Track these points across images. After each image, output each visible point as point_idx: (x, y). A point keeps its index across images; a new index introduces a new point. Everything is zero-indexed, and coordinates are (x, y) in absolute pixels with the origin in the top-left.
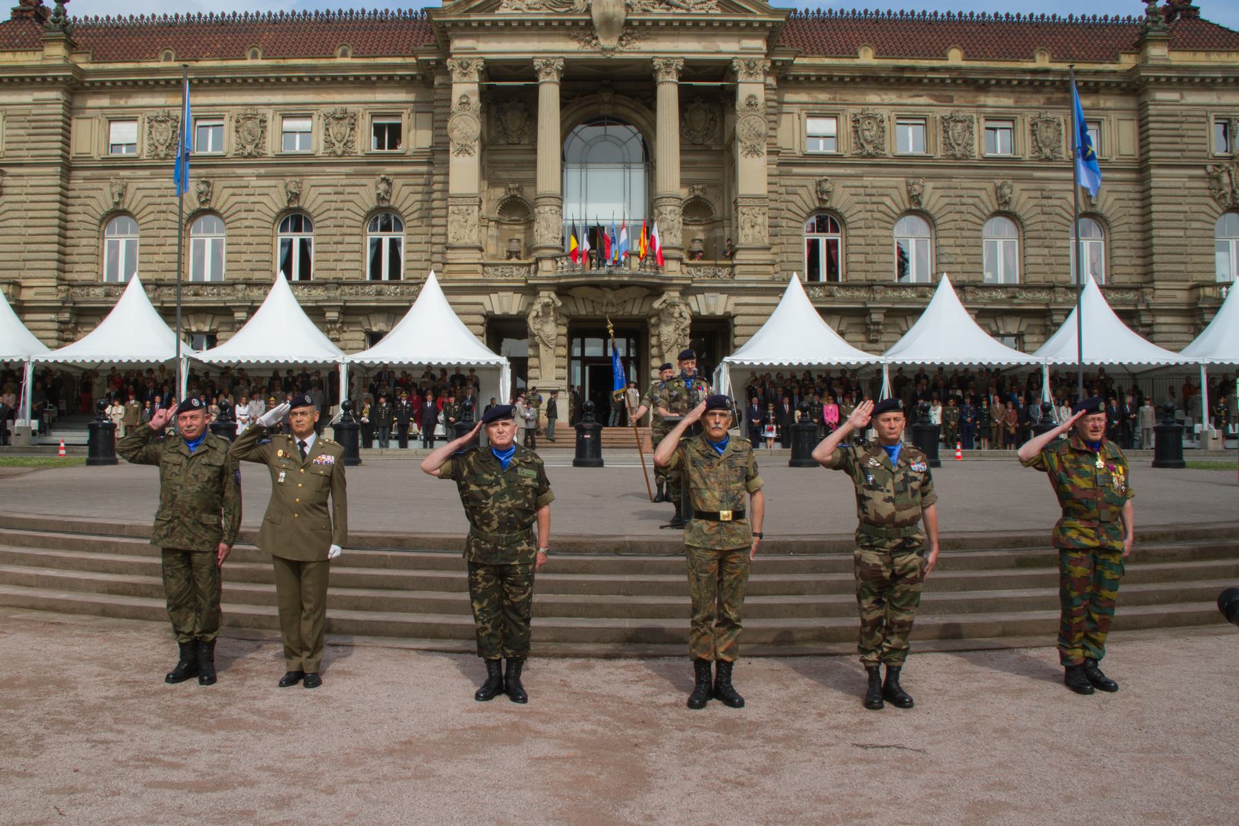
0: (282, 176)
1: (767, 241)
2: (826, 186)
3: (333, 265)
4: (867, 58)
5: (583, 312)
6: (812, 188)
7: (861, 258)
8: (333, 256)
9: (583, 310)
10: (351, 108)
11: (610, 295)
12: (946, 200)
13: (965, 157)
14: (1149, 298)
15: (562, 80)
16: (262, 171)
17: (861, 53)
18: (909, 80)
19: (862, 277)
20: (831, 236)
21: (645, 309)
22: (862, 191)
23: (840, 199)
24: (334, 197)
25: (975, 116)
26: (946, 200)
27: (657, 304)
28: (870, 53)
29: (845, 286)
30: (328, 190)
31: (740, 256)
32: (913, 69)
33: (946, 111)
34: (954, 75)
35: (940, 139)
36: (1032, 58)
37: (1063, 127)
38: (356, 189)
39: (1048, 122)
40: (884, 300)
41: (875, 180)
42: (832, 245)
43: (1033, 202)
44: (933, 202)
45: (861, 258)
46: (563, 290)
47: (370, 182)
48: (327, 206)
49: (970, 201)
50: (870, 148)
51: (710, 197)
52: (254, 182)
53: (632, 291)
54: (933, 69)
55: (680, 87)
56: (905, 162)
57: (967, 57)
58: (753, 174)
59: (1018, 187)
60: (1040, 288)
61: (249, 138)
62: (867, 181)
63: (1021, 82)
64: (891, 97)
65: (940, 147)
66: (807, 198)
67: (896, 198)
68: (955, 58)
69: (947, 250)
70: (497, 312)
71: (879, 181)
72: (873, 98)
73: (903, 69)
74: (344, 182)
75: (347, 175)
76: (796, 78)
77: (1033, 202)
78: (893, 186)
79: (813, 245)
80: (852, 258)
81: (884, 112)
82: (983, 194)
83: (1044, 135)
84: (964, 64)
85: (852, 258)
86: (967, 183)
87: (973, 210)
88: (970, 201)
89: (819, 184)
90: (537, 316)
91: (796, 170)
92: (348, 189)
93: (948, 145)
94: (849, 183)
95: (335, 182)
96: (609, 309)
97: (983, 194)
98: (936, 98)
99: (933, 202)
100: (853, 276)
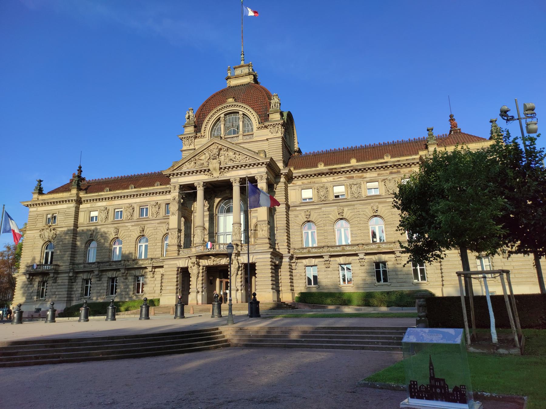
6: (303, 214)
10: (159, 202)
12: (353, 214)
15: (205, 189)
16: (133, 224)
17: (319, 165)
18: (335, 173)
22: (322, 213)
25: (362, 182)
26: (353, 214)
28: (323, 165)
32: (336, 169)
33: (351, 181)
34: (352, 168)
35: (349, 192)
41: (326, 209)
43: (387, 211)
44: (348, 214)
49: (362, 213)
50: (323, 198)
54: (343, 168)
57: (357, 161)
59: (380, 206)
60: (391, 243)
63: (377, 168)
64: (330, 178)
65: (349, 194)
68: (353, 162)
69: (354, 232)
71: (328, 209)
72: (324, 179)
73: (332, 169)
77: (387, 211)
78: (333, 211)
82: (367, 210)
83: (389, 185)
84: (357, 164)
86: (361, 207)
87: (364, 216)
88: (362, 213)
91: (298, 208)
97: (367, 210)
98: (348, 178)
99: (348, 214)
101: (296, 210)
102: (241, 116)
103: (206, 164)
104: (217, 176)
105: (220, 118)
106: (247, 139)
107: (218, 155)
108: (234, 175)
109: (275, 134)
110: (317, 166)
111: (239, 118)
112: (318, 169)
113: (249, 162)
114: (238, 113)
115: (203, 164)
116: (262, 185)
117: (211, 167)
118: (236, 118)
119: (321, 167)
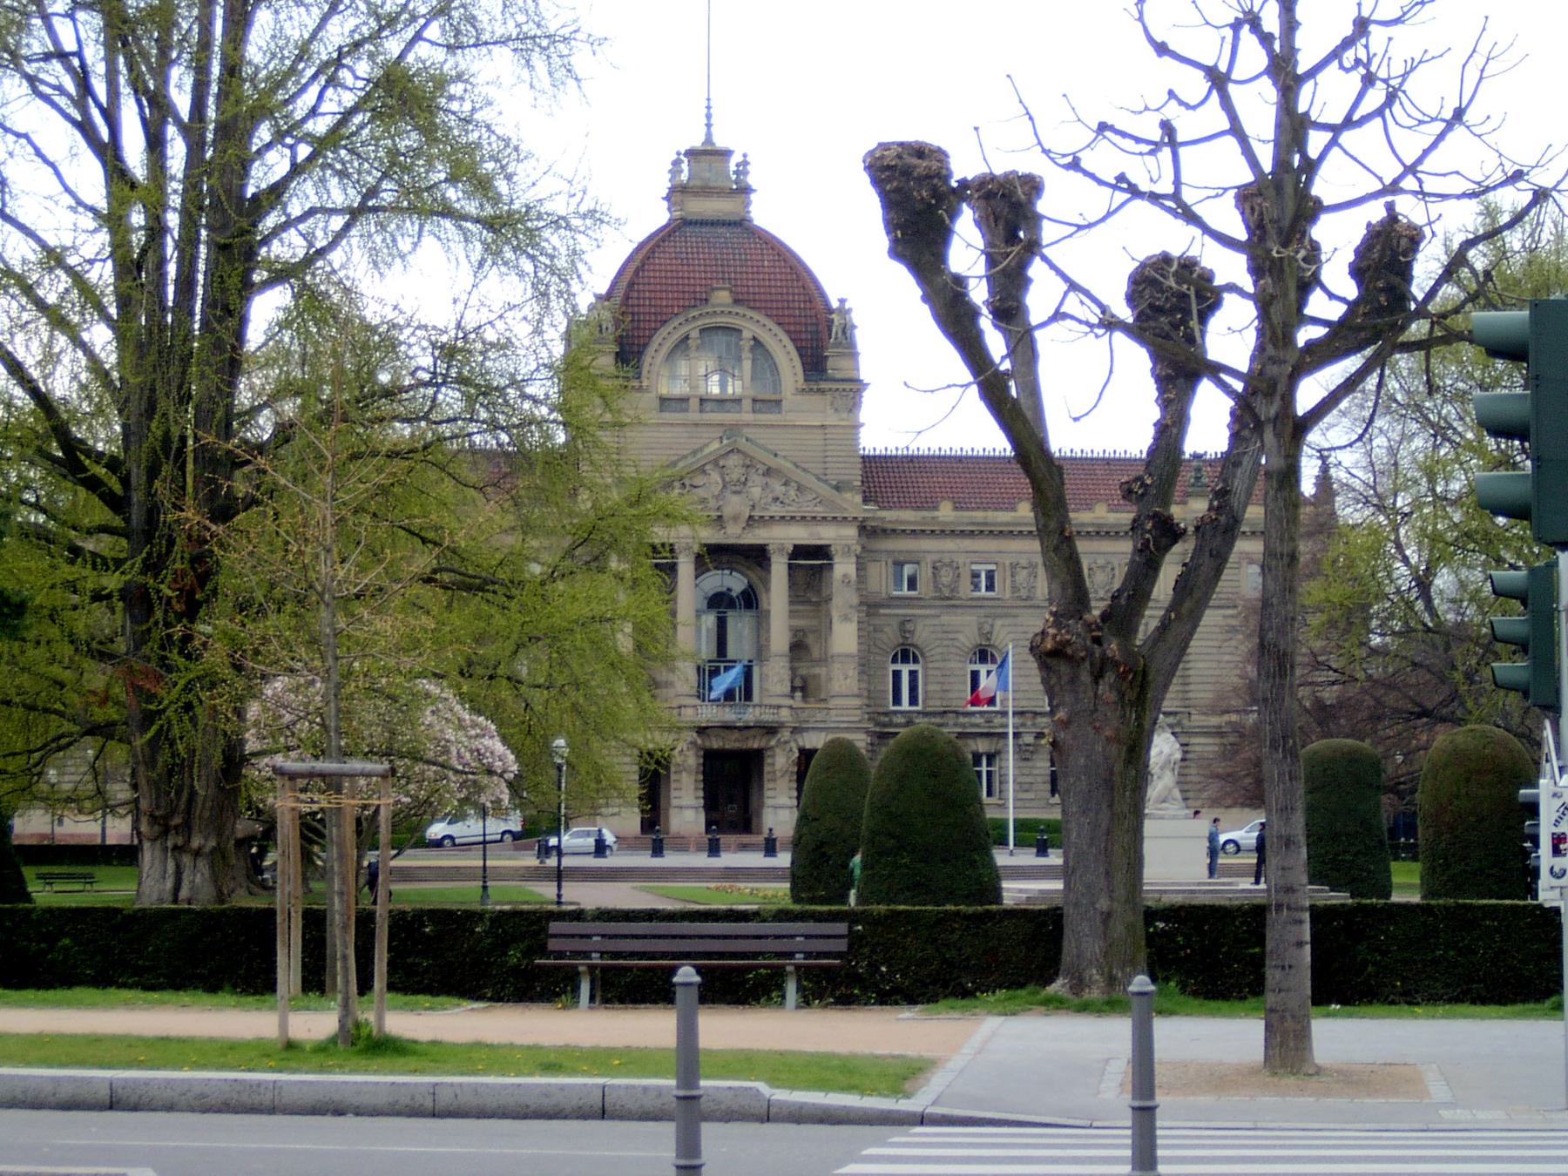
1: (856, 691)
2: (909, 626)
4: (946, 512)
5: (715, 746)
6: (896, 627)
7: (937, 687)
9: (716, 744)
11: (736, 734)
13: (1028, 598)
14: (1185, 722)
19: (938, 703)
20: (913, 667)
21: (763, 744)
22: (939, 629)
23: (922, 634)
27: (773, 743)
29: (925, 714)
31: (833, 703)
35: (1008, 582)
36: (1089, 508)
37: (1117, 572)
39: (1103, 568)
40: (956, 725)
42: (913, 674)
45: (937, 687)
46: (701, 731)
51: (810, 640)
53: (752, 732)
55: (790, 566)
56: (975, 604)
58: (845, 637)
62: (945, 619)
66: (890, 637)
67: (968, 638)
76: (884, 530)
79: (897, 675)
80: (930, 688)
81: (960, 559)
85: (930, 688)
89: (903, 623)
91: (882, 611)
93: (1015, 588)
94: (928, 622)
96: (731, 743)
100: (931, 703)
101: (877, 615)
102: (746, 345)
103: (712, 503)
104: (734, 534)
105: (687, 338)
106: (760, 411)
107: (744, 484)
108: (782, 537)
109: (844, 415)
110: (936, 508)
111: (740, 349)
112: (936, 513)
113: (820, 511)
114: (740, 331)
115: (703, 501)
116: (843, 568)
117: (727, 511)
118: (728, 345)
119: (946, 512)
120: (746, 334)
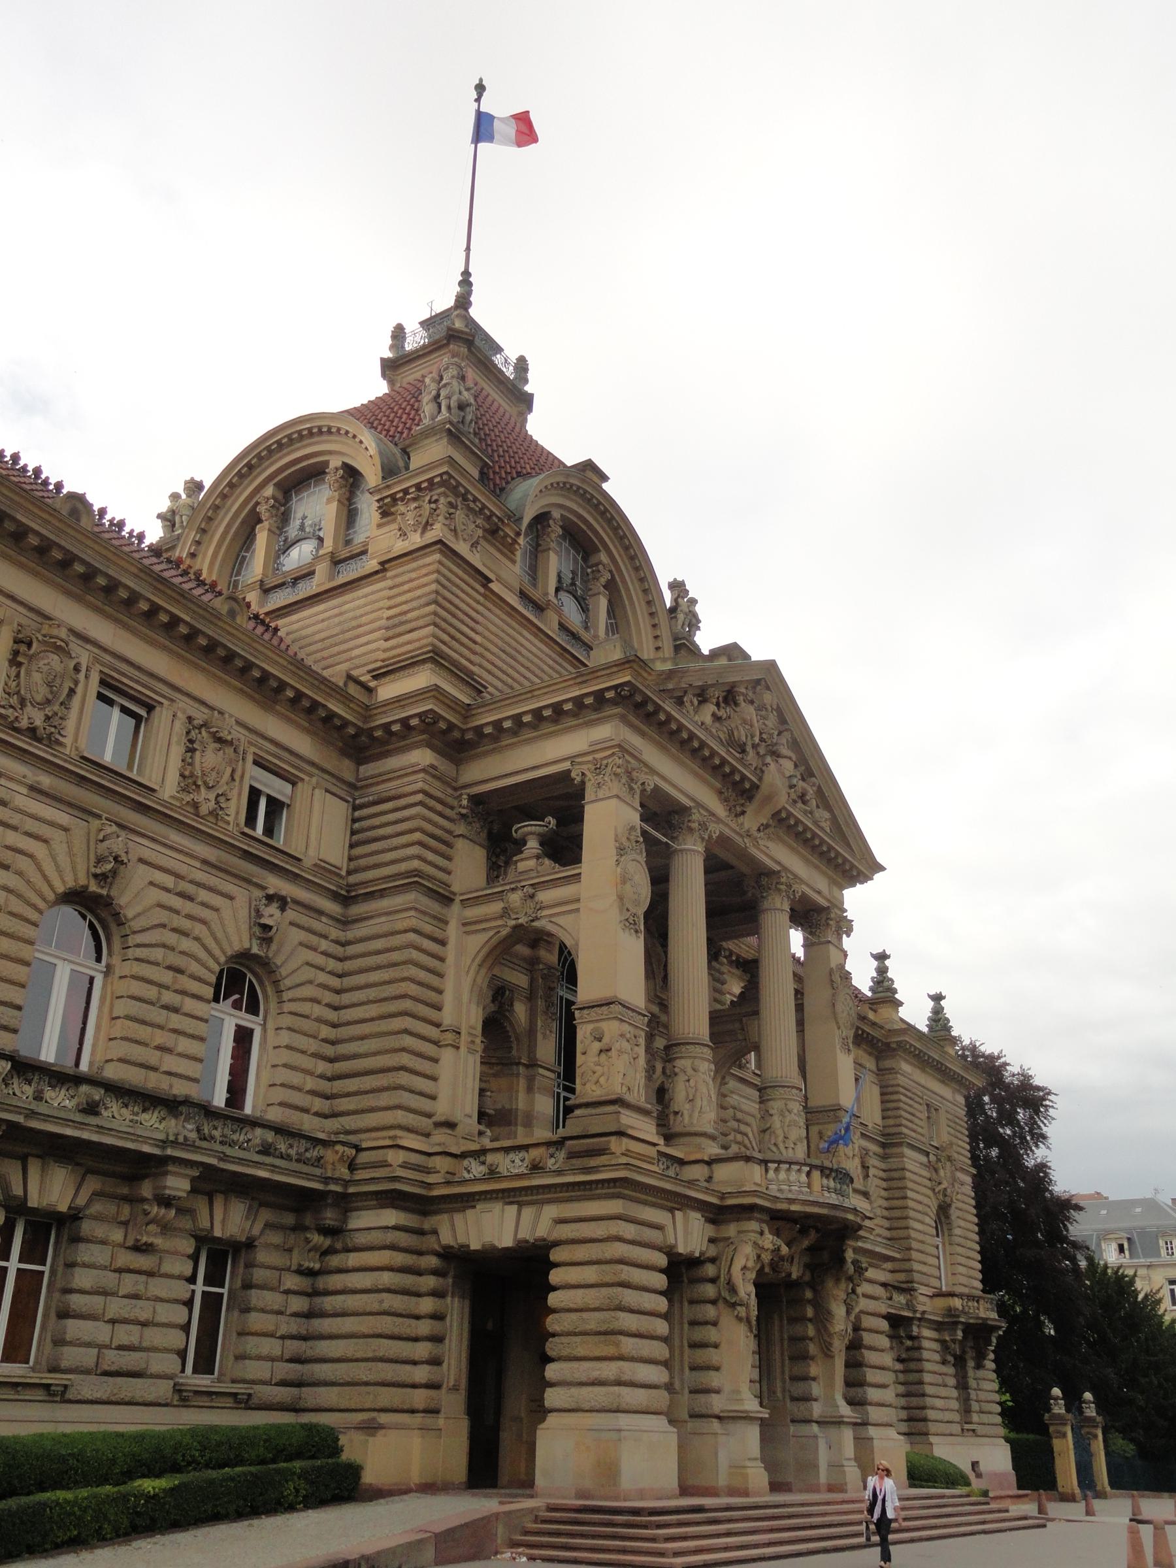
0: (87, 813)
3: (153, 1057)
8: (160, 1038)
24: (176, 902)
30: (169, 881)
38: (216, 900)
47: (241, 894)
48: (162, 916)
52: (22, 800)
61: (41, 693)
70: (681, 1249)
74: (200, 876)
75: (205, 862)
90: (744, 1268)
92: (203, 895)
95: (183, 869)
120: (603, 557)
